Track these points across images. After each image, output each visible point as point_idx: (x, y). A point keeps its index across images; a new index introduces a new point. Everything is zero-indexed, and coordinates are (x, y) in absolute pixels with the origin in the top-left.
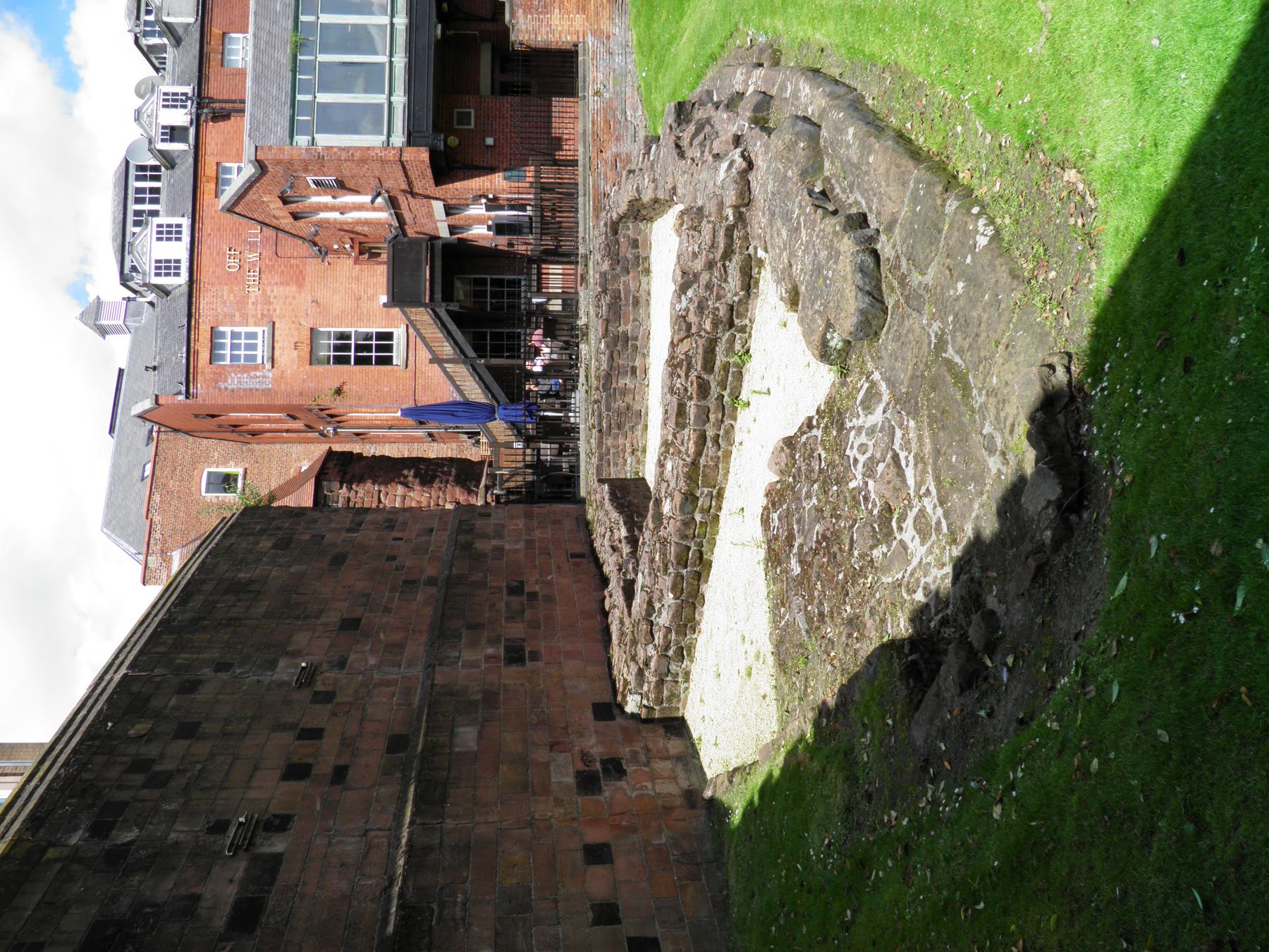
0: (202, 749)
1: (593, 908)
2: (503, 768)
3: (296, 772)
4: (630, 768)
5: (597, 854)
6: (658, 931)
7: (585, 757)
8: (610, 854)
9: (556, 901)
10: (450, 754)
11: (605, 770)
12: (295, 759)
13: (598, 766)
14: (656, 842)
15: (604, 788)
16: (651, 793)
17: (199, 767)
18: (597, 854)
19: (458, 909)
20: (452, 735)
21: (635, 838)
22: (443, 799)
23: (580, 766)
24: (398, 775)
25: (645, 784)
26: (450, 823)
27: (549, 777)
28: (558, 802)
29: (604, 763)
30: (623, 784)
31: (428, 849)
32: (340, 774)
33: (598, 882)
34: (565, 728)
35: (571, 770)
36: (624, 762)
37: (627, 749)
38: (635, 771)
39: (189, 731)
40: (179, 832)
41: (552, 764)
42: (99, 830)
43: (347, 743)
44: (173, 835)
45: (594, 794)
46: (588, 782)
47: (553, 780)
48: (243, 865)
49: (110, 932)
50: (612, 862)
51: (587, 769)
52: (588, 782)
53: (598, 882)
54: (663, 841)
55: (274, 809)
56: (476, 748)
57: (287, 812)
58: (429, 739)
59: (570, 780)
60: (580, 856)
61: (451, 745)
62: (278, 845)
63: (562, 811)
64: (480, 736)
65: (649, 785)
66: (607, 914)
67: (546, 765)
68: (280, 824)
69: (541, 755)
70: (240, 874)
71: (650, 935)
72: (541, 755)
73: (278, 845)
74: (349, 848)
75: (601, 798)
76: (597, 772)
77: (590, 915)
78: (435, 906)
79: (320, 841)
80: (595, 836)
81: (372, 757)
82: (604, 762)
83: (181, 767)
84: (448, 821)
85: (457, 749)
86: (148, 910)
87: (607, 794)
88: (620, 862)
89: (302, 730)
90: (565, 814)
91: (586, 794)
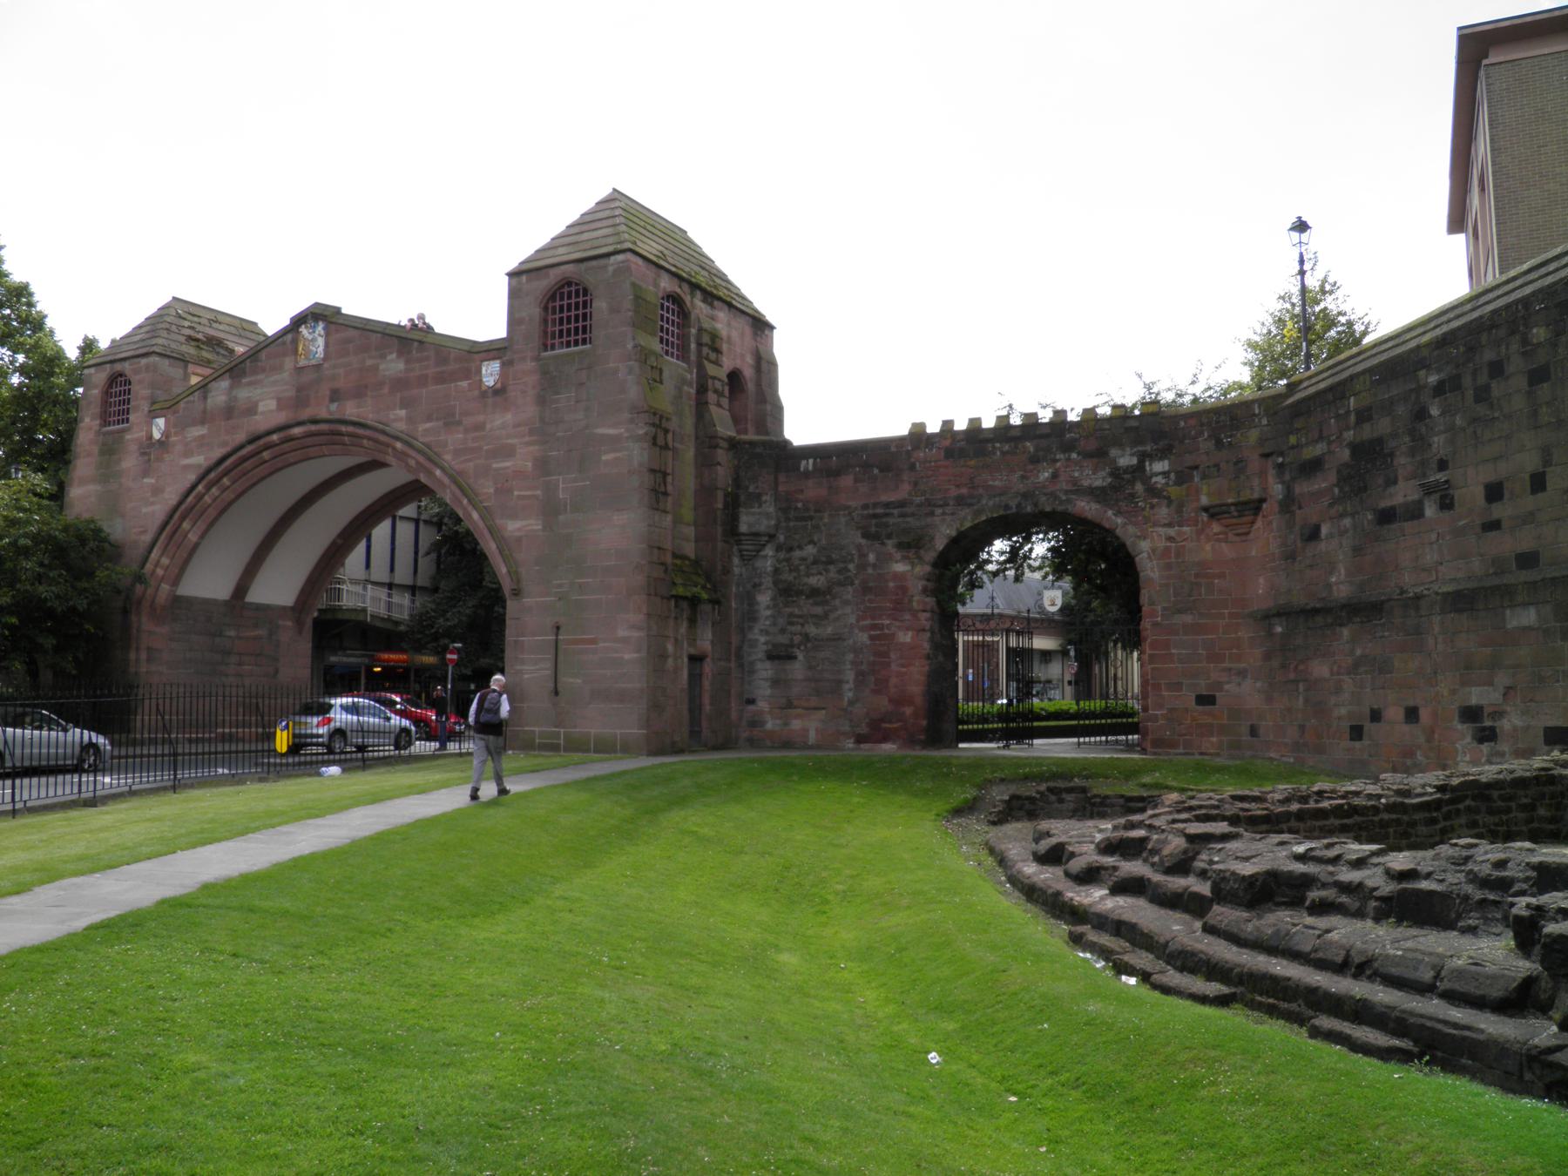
0: (1519, 403)
1: (1379, 709)
2: (1488, 650)
3: (1494, 492)
4: (1485, 748)
5: (1412, 714)
6: (1366, 742)
7: (1498, 714)
8: (1412, 723)
9: (1383, 688)
10: (1502, 607)
11: (1484, 729)
12: (1506, 485)
13: (1488, 723)
14: (1419, 753)
15: (1465, 726)
16: (1459, 759)
17: (1496, 415)
18: (1412, 714)
19: (1381, 634)
20: (1525, 605)
21: (1422, 740)
22: (1459, 611)
23: (1487, 711)
24: (1491, 571)
25: (1468, 755)
26: (1436, 619)
27: (1479, 685)
28: (1453, 692)
29: (1492, 729)
30: (1468, 739)
31: (1417, 609)
32: (1493, 526)
33: (1394, 713)
34: (1531, 700)
35: (1483, 702)
36: (1493, 744)
37: (1506, 749)
38: (1481, 751)
39: (1538, 376)
40: (1439, 443)
41: (1491, 689)
42: (1439, 390)
43: (1529, 518)
44: (1436, 439)
45: (1460, 717)
46: (1471, 714)
47: (1473, 689)
48: (1416, 497)
49: (1378, 449)
50: (1406, 723)
51: (1485, 715)
52: (1471, 714)
53: (1394, 713)
54: (1420, 758)
55: (1457, 494)
56: (1509, 626)
57: (1456, 505)
58: (1520, 587)
59: (1474, 701)
60: (1411, 703)
61: (1512, 607)
62: (1430, 511)
63: (1446, 694)
64: (1530, 628)
65: (1467, 758)
66: (1376, 716)
67: (1491, 684)
68: (1446, 504)
69: (1502, 679)
70: (1410, 498)
71: (1364, 738)
72: (1502, 679)
73: (1430, 511)
74: (1428, 557)
75: (1455, 723)
76: (1483, 722)
77: (1376, 707)
78: (1383, 620)
79: (1434, 536)
80: (1424, 714)
81: (1506, 544)
82: (1492, 729)
83: (1495, 401)
84: (1439, 618)
85: (1508, 612)
86: (1389, 460)
87: (1460, 727)
88: (1406, 728)
89: (1544, 472)
90: (1442, 696)
91: (1460, 712)
